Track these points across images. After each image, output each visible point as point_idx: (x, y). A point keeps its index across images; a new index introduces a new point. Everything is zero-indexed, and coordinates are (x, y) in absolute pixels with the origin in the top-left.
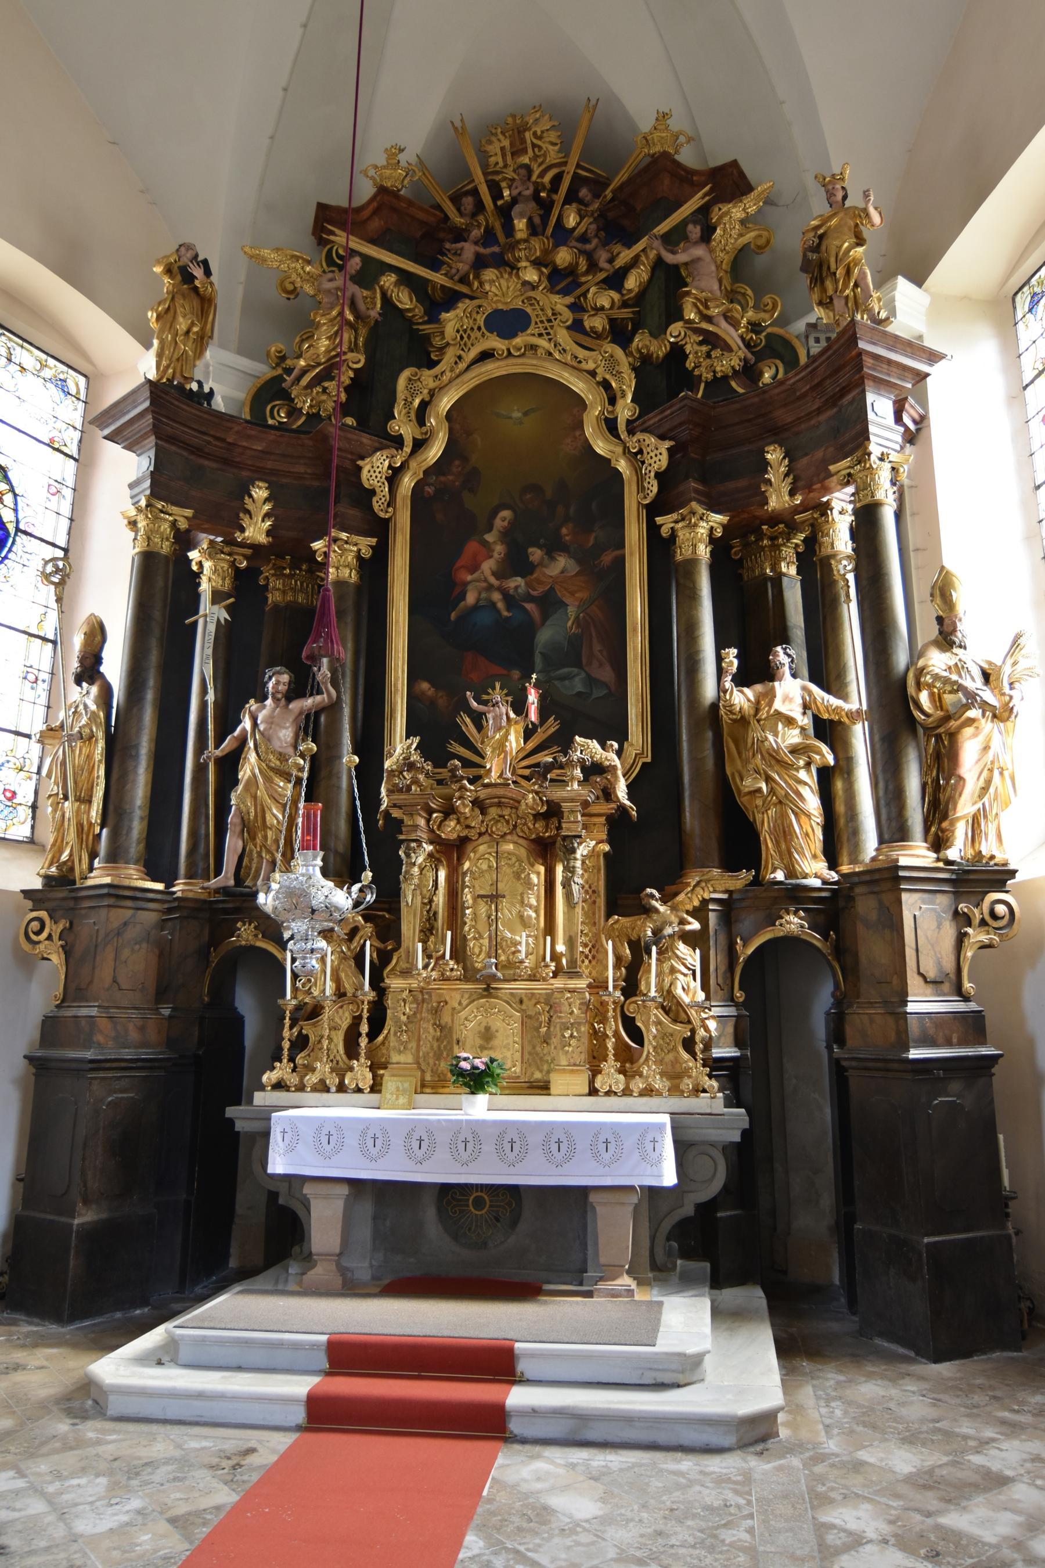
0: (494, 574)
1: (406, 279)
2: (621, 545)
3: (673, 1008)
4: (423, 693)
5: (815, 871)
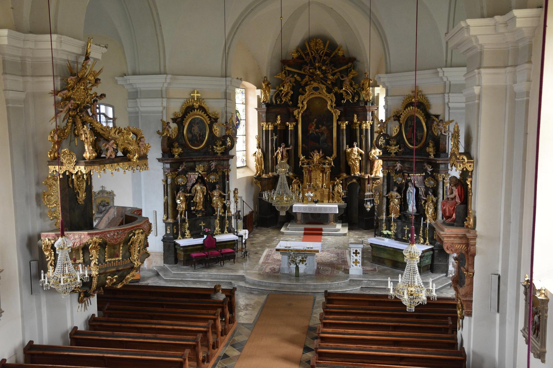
1: (299, 74)
3: (338, 192)
5: (358, 173)
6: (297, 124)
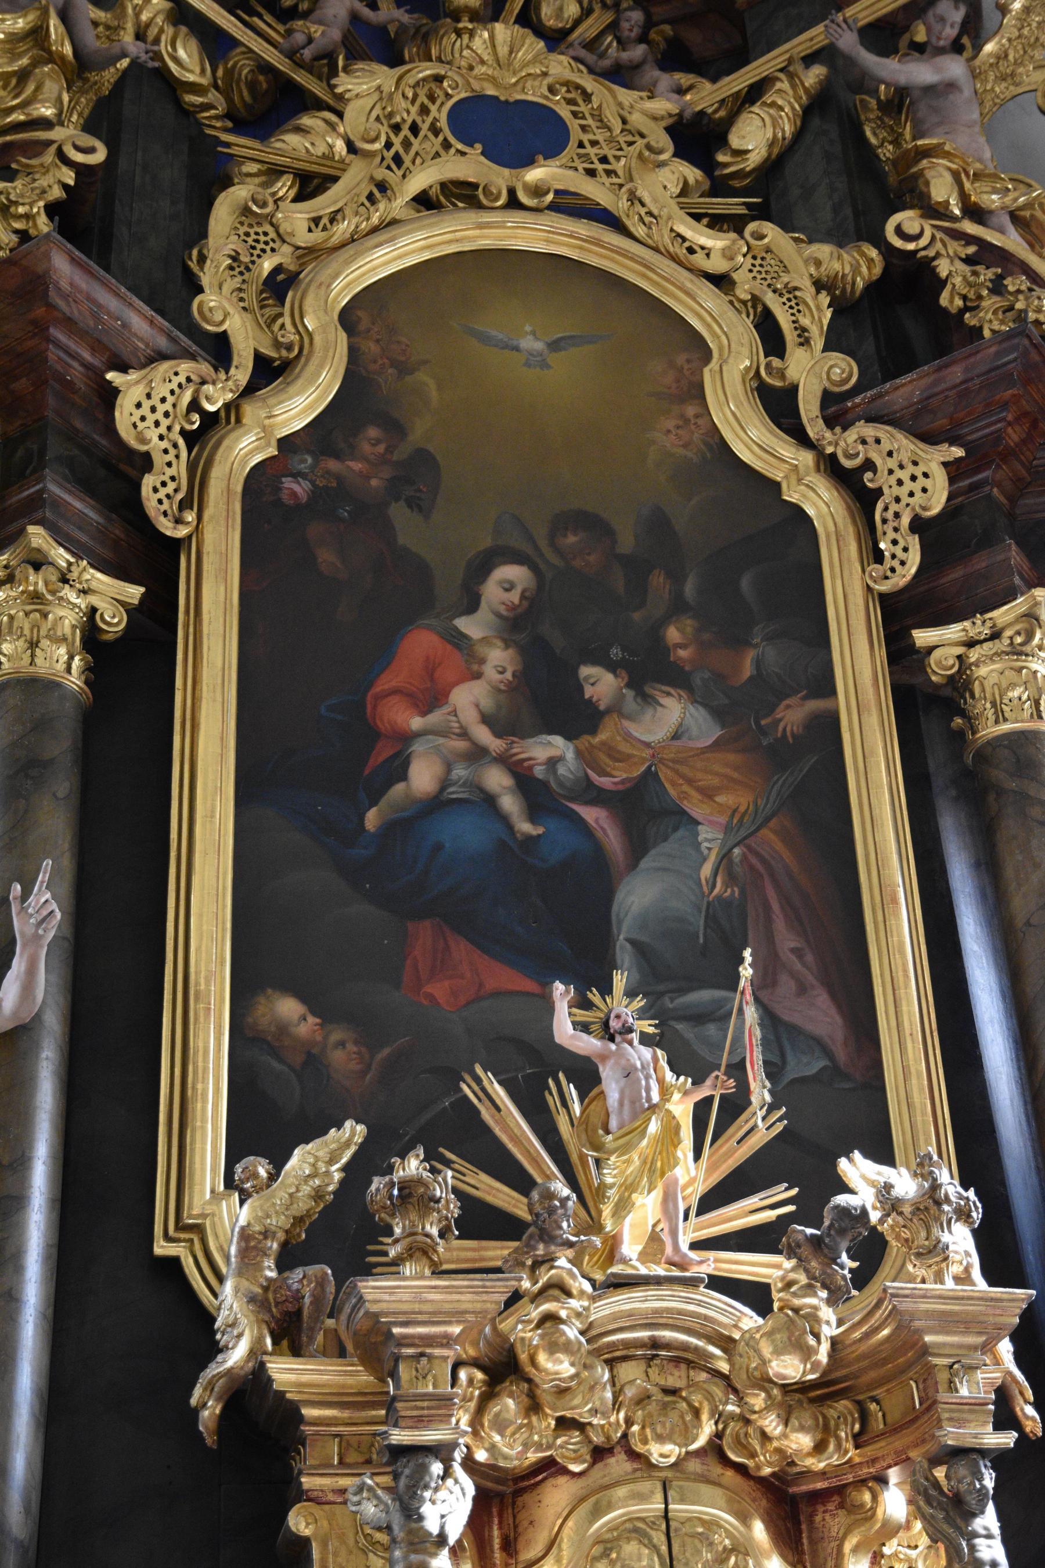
0: (486, 719)
2: (825, 686)
4: (283, 1029)
6: (156, 627)
